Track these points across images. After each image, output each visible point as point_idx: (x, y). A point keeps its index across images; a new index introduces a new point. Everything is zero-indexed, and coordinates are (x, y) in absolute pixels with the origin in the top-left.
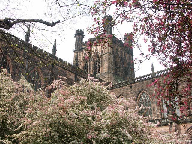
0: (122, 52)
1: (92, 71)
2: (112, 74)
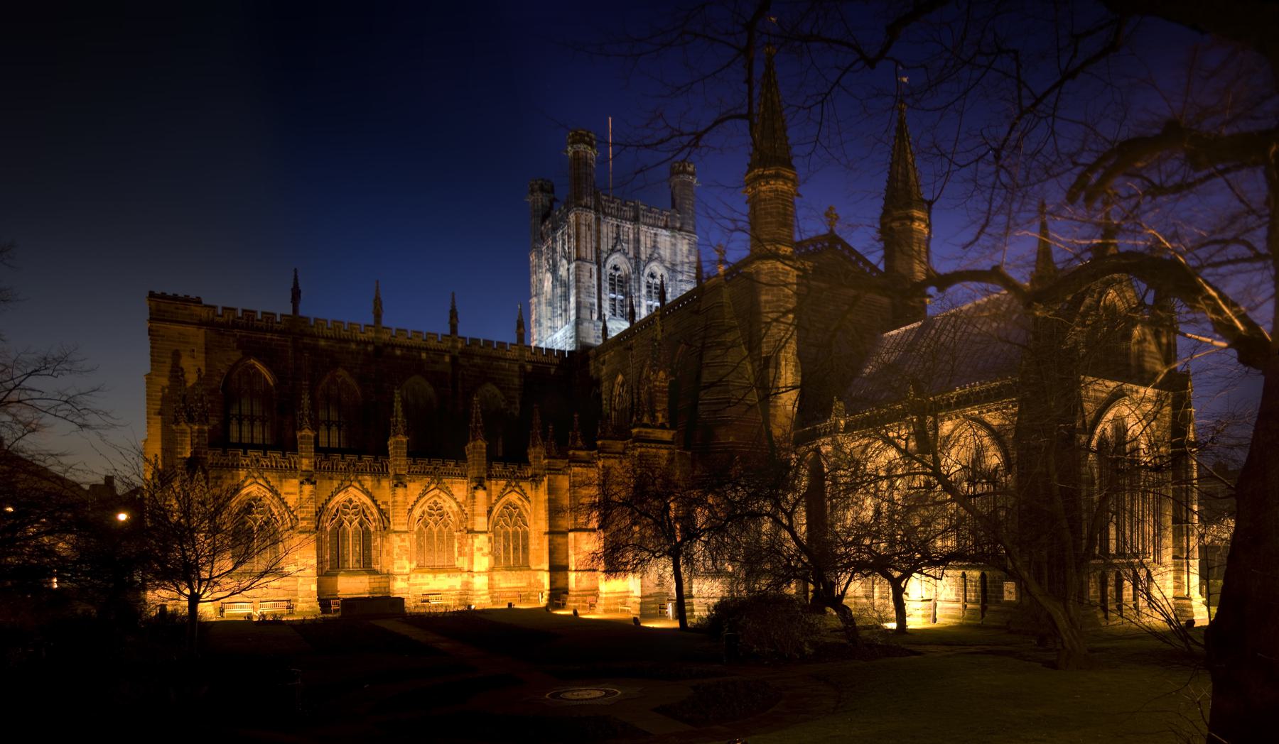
0: (637, 241)
1: (561, 315)
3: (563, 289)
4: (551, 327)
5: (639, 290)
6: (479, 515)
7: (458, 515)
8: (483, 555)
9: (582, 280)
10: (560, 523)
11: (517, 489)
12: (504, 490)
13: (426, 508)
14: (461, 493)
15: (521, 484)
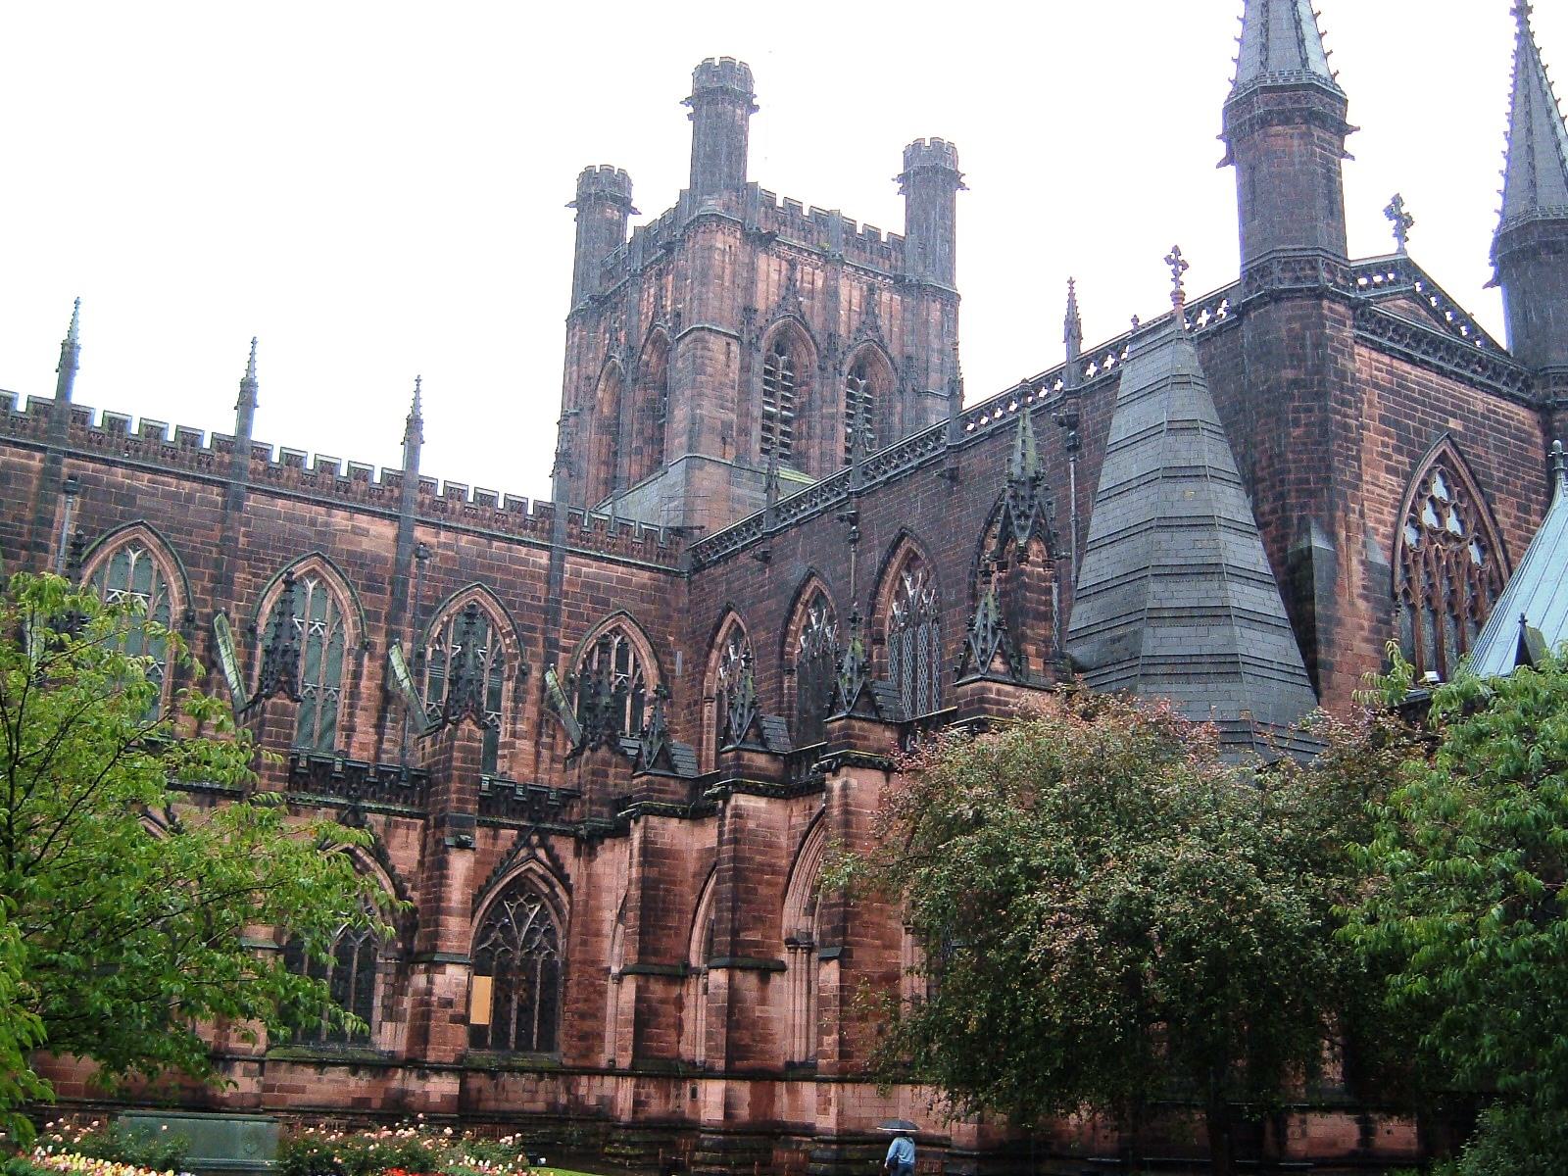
0: (832, 293)
1: (639, 451)
9: (709, 370)
10: (665, 943)
11: (541, 853)
14: (401, 854)
15: (552, 840)
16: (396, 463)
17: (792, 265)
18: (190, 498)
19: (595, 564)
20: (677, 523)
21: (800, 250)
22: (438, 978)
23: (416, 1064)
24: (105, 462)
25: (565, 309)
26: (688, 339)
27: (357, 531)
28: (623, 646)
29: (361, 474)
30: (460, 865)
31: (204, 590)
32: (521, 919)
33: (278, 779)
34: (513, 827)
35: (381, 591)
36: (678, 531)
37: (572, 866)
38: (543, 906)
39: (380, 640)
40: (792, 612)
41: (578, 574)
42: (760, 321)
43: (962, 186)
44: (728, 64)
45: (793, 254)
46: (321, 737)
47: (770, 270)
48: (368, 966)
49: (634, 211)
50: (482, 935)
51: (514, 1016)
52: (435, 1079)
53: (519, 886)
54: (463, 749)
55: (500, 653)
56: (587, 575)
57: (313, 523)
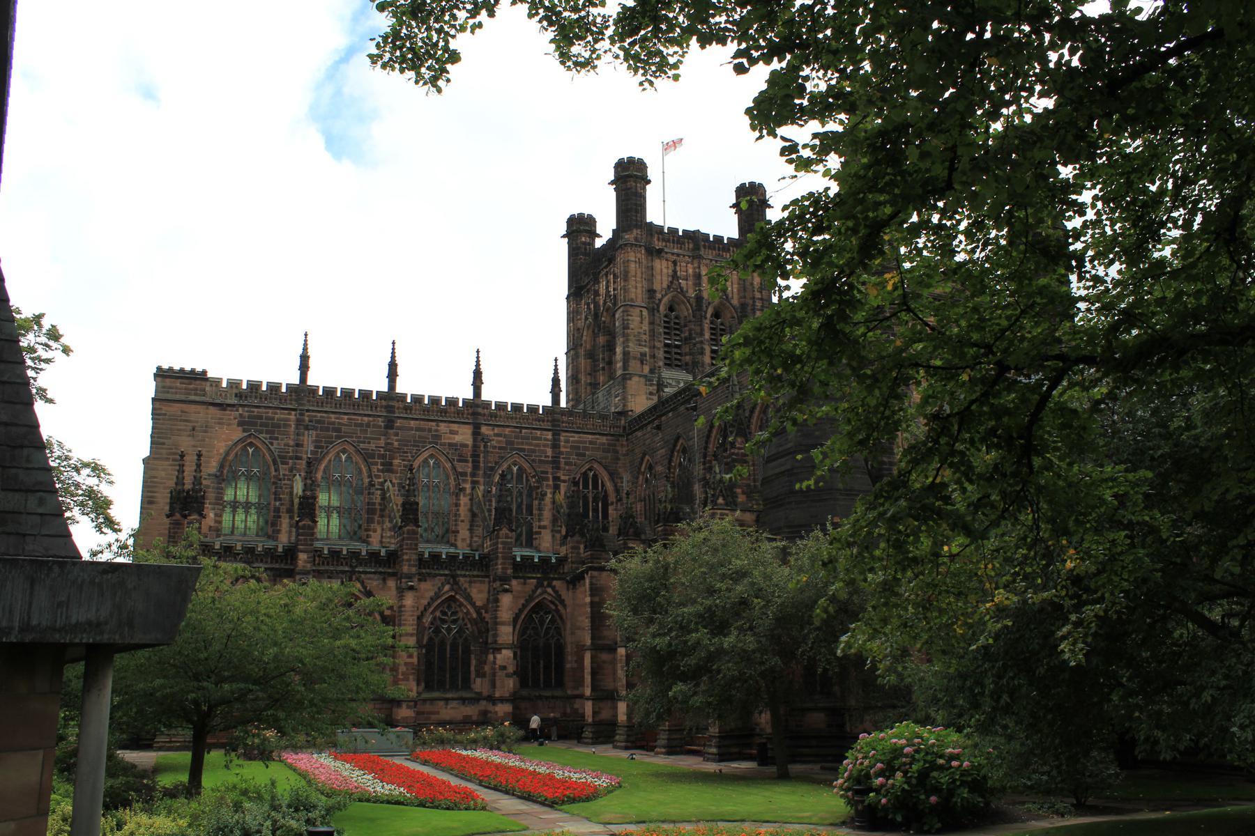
1: (603, 369)
2: (640, 376)
3: (607, 338)
4: (590, 384)
5: (702, 334)
6: (503, 624)
7: (476, 624)
8: (508, 676)
9: (631, 326)
10: (606, 633)
11: (549, 590)
12: (534, 592)
13: (438, 614)
14: (480, 596)
15: (555, 583)
16: (470, 396)
17: (675, 263)
18: (368, 425)
19: (576, 435)
20: (618, 410)
21: (678, 255)
22: (498, 656)
23: (492, 699)
24: (326, 412)
25: (566, 293)
26: (621, 309)
27: (452, 432)
28: (595, 476)
29: (452, 402)
30: (506, 600)
31: (378, 470)
32: (542, 622)
33: (414, 566)
34: (533, 578)
35: (467, 461)
36: (620, 413)
37: (566, 595)
38: (553, 616)
39: (468, 486)
40: (672, 456)
41: (567, 441)
42: (659, 296)
43: (770, 206)
44: (631, 160)
45: (675, 257)
46: (443, 537)
47: (662, 268)
48: (467, 651)
49: (599, 236)
50: (523, 632)
51: (542, 670)
52: (500, 705)
53: (539, 606)
54: (503, 543)
55: (530, 486)
56: (573, 442)
57: (430, 430)
